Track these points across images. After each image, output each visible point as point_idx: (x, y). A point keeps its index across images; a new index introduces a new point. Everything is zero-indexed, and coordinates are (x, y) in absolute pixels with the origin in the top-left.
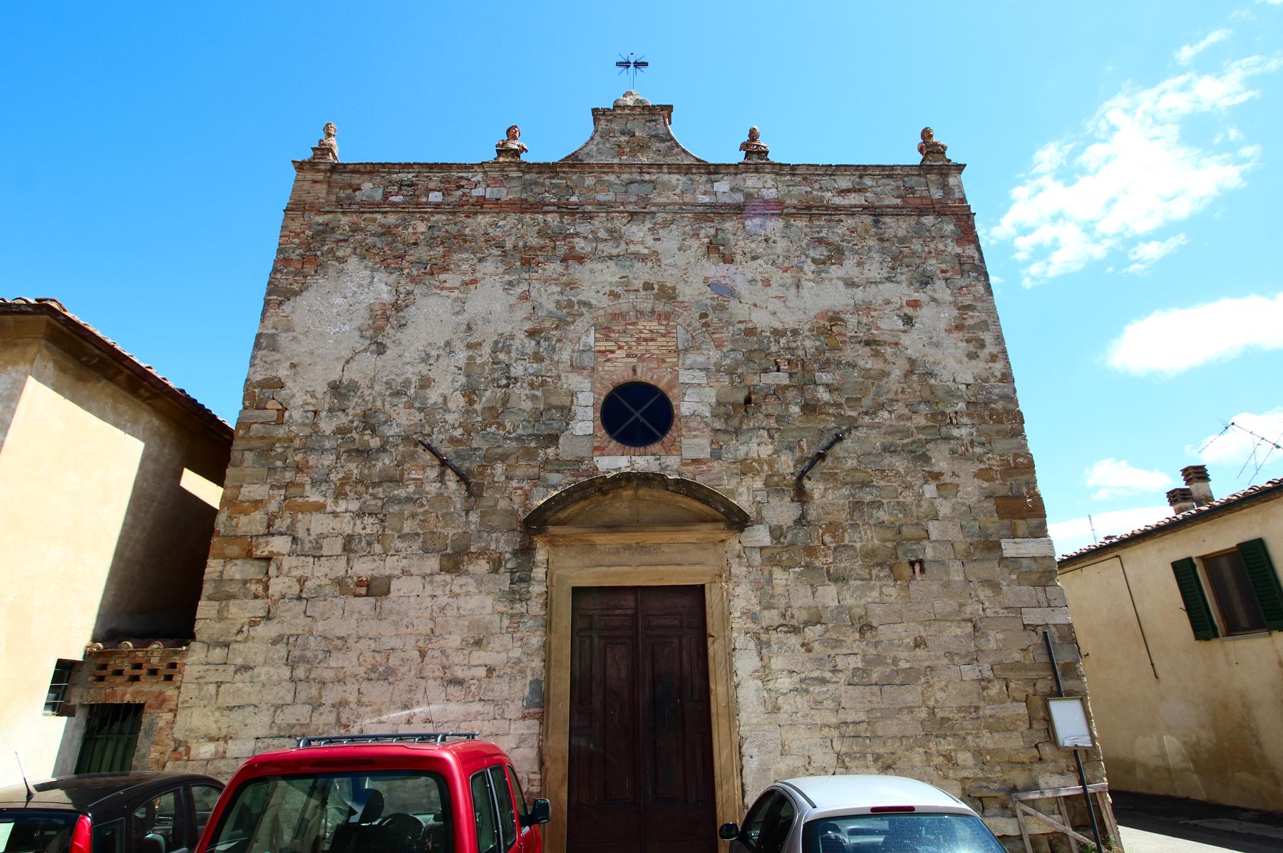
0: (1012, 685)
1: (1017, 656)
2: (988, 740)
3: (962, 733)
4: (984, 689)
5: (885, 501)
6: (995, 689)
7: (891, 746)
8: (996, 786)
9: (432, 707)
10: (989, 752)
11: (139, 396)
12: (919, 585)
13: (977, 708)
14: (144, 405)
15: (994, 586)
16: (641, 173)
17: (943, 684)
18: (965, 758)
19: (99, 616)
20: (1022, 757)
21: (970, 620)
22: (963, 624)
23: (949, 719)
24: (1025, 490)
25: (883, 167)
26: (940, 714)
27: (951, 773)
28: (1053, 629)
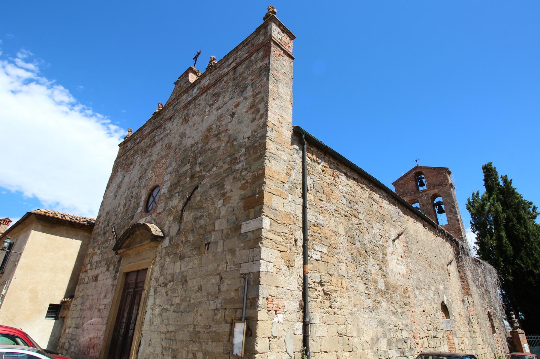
0: (227, 313)
1: (233, 294)
3: (202, 341)
4: (215, 315)
11: (77, 228)
13: (210, 326)
15: (232, 251)
17: (202, 311)
22: (216, 277)
24: (258, 189)
25: (243, 43)
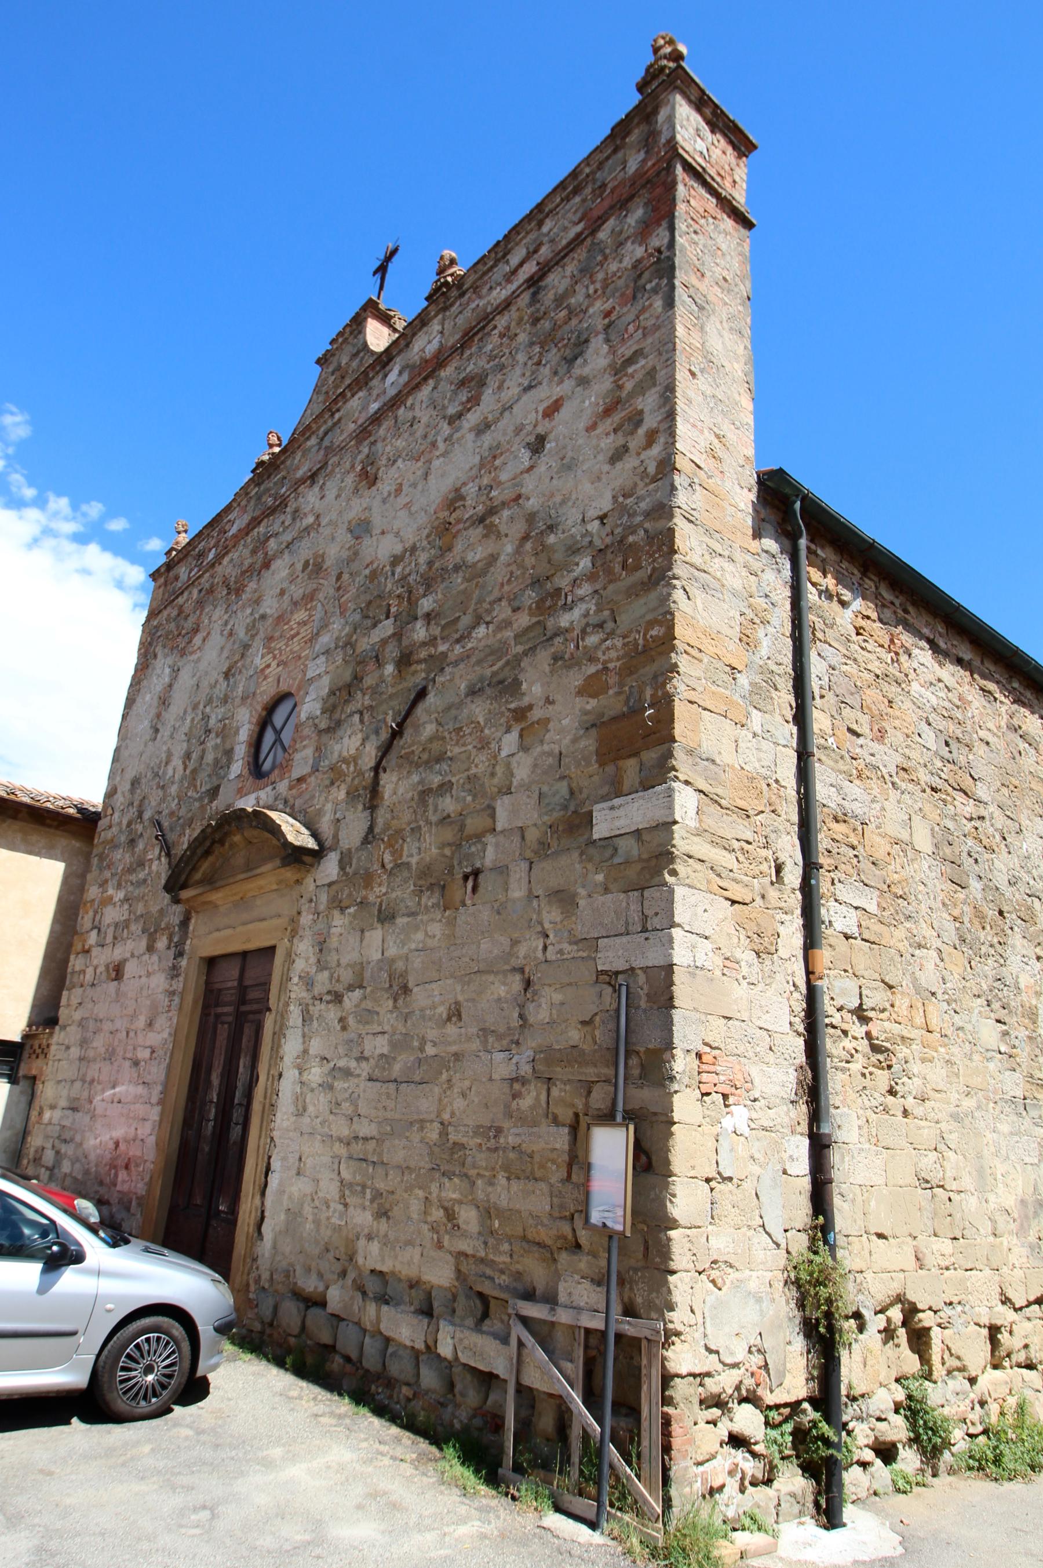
0: (555, 1092)
1: (575, 1035)
2: (505, 1193)
3: (473, 1172)
4: (515, 1096)
5: (454, 780)
6: (531, 1098)
7: (394, 1179)
8: (503, 1279)
9: (117, 1090)
10: (500, 1213)
11: (50, 826)
12: (476, 913)
13: (499, 1131)
14: (58, 832)
15: (564, 898)
16: (333, 415)
17: (467, 1083)
18: (469, 1217)
19: (34, 1006)
20: (544, 1235)
21: (522, 970)
22: (510, 977)
23: (463, 1146)
24: (648, 692)
25: (561, 186)
26: (452, 1137)
27: (446, 1240)
28: (642, 978)
